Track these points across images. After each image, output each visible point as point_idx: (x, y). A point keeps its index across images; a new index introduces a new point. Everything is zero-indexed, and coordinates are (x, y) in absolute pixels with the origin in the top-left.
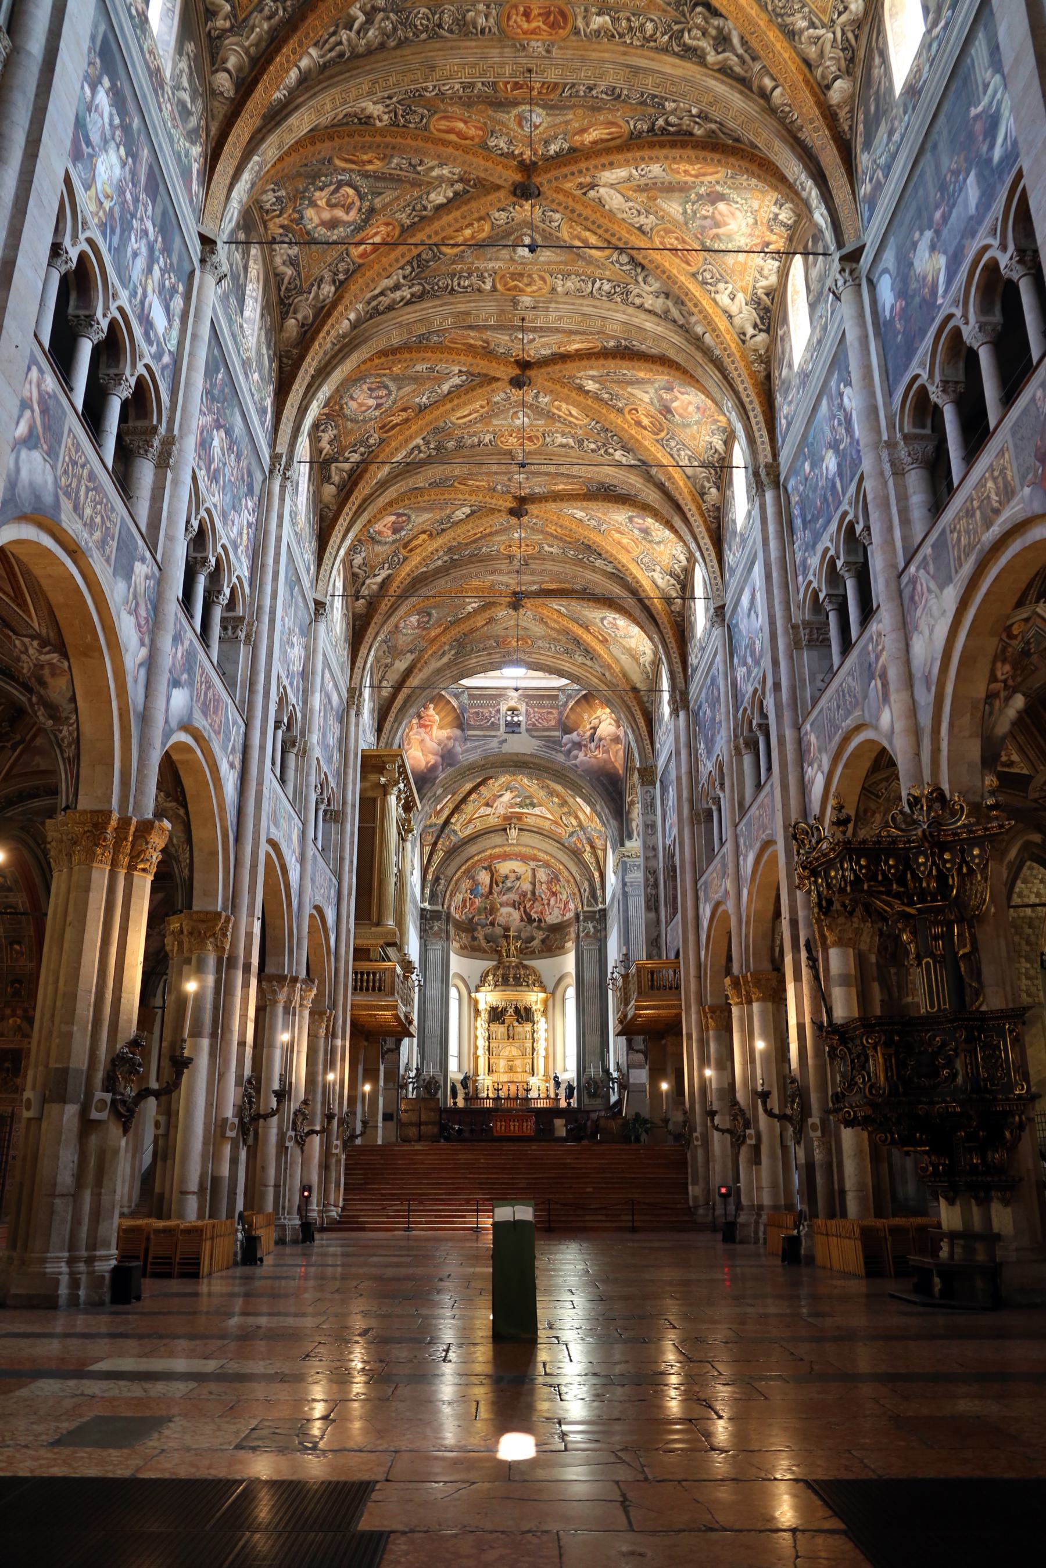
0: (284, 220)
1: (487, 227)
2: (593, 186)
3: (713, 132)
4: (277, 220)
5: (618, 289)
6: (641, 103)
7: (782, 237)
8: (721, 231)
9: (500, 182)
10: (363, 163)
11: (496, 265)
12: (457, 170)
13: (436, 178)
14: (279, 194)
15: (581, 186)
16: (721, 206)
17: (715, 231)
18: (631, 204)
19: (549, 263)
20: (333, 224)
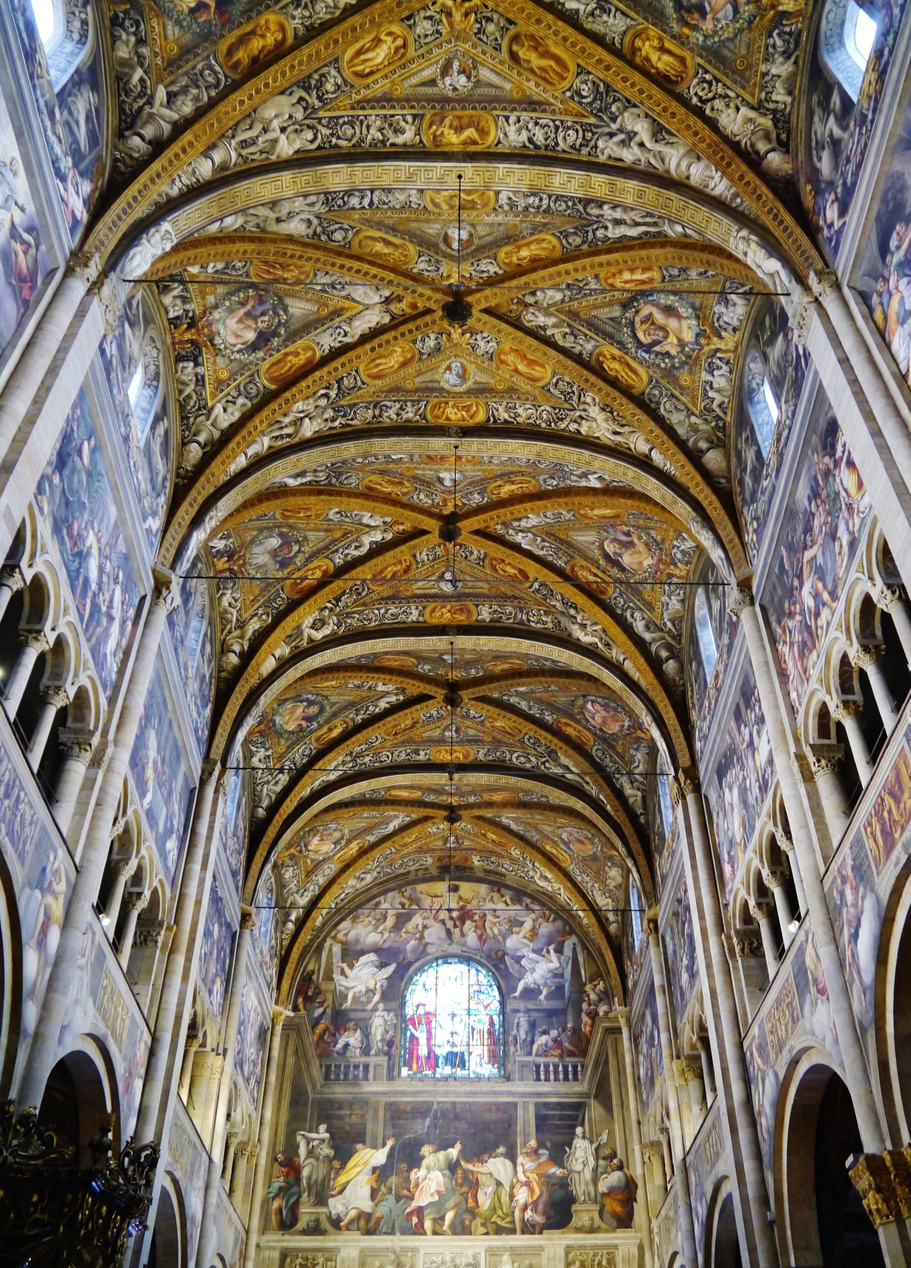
0: (716, 343)
1: (502, 255)
2: (387, 301)
3: (285, 415)
4: (723, 347)
5: (340, 202)
6: (355, 405)
7: (181, 342)
8: (242, 311)
9: (485, 317)
10: (620, 360)
11: (492, 218)
12: (529, 317)
13: (552, 315)
14: (709, 378)
15: (399, 299)
16: (251, 336)
17: (249, 307)
18: (344, 293)
19: (428, 221)
20: (669, 311)
